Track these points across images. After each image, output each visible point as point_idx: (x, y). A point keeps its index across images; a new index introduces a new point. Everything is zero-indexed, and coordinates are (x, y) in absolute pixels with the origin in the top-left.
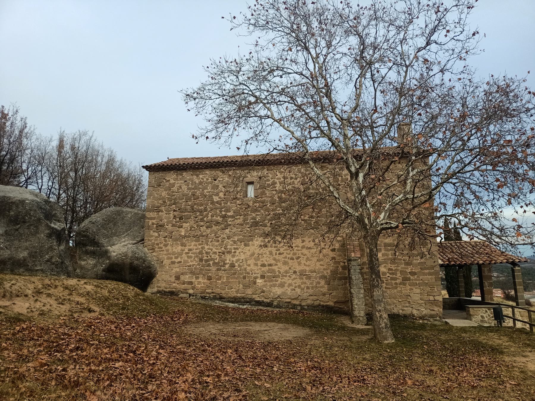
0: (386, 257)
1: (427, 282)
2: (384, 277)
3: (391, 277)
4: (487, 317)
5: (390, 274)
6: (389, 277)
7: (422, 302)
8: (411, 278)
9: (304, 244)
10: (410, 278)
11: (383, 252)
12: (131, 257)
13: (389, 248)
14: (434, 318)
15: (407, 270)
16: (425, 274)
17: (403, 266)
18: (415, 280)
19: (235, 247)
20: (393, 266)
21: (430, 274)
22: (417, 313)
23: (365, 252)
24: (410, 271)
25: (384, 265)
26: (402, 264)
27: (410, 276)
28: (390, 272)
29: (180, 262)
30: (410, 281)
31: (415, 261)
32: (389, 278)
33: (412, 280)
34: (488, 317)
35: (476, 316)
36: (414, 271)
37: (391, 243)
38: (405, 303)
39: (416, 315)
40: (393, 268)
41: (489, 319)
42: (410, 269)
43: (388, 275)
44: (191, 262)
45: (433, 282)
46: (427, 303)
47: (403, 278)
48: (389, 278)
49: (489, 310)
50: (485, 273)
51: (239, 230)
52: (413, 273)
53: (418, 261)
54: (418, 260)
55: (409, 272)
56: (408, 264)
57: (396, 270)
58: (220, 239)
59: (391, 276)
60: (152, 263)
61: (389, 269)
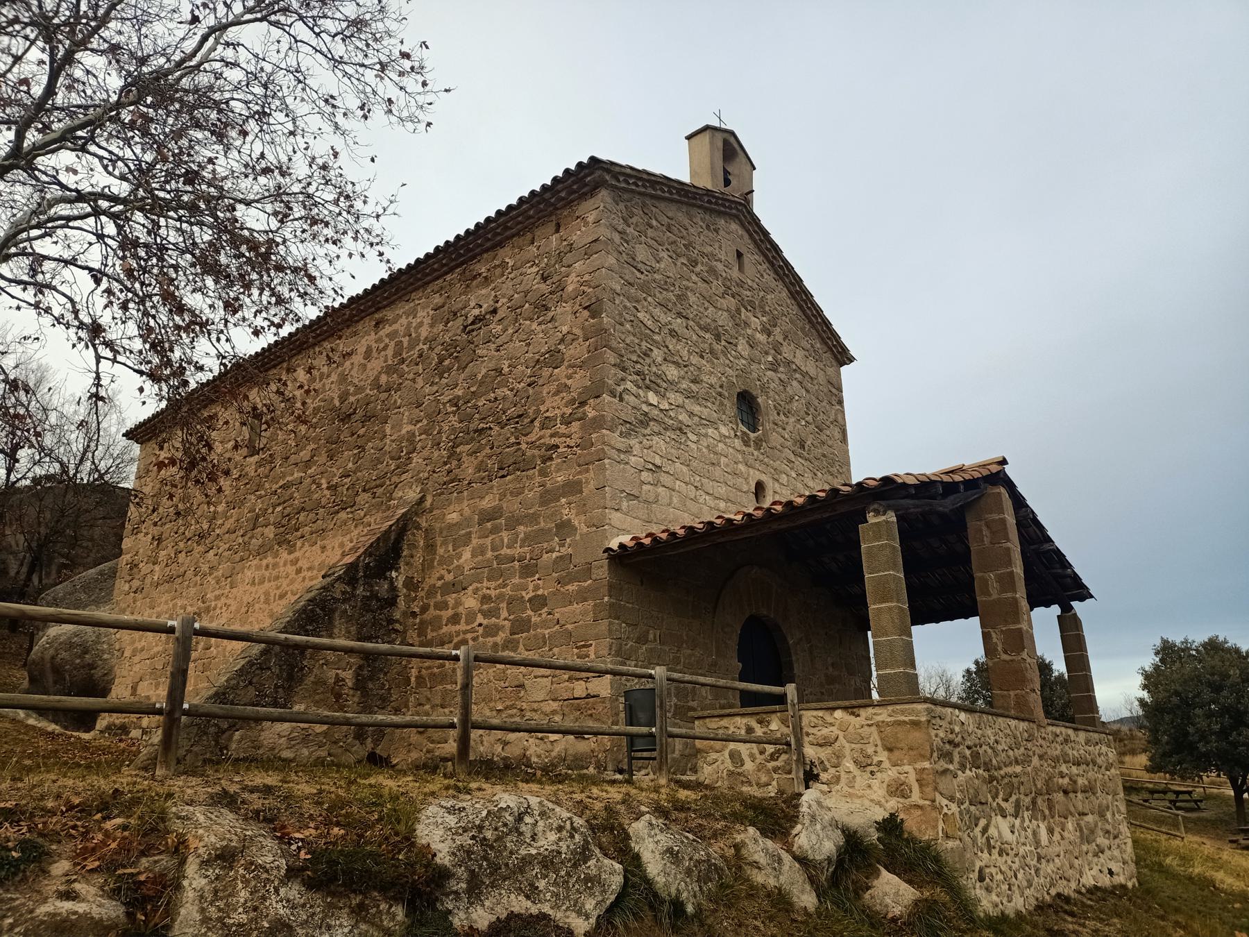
0: (480, 557)
1: (570, 627)
2: (469, 627)
3: (487, 627)
4: (753, 760)
5: (486, 614)
6: (480, 625)
7: (555, 705)
8: (533, 619)
9: (324, 556)
10: (529, 618)
11: (475, 541)
12: (61, 643)
13: (489, 525)
14: (583, 768)
15: (524, 593)
16: (569, 600)
17: (516, 580)
18: (544, 625)
19: (217, 593)
20: (493, 584)
21: (582, 596)
22: (539, 751)
23: (435, 554)
24: (531, 594)
25: (475, 585)
26: (512, 575)
27: (529, 612)
28: (485, 607)
29: (142, 649)
30: (528, 631)
31: (545, 556)
32: (481, 630)
33: (536, 626)
34: (760, 758)
35: (714, 756)
36: (540, 592)
37: (494, 508)
38: (512, 716)
39: (534, 759)
40: (493, 593)
41: (760, 767)
42: (531, 587)
43: (480, 619)
44: (157, 645)
45: (586, 626)
46: (566, 710)
47: (513, 622)
48: (481, 630)
49: (760, 722)
50: (990, 595)
51: (228, 545)
52: (539, 602)
53: (554, 555)
54: (552, 551)
55: (530, 600)
56: (528, 570)
57: (500, 597)
58: (198, 578)
59: (485, 622)
60: (105, 656)
61: (486, 599)
